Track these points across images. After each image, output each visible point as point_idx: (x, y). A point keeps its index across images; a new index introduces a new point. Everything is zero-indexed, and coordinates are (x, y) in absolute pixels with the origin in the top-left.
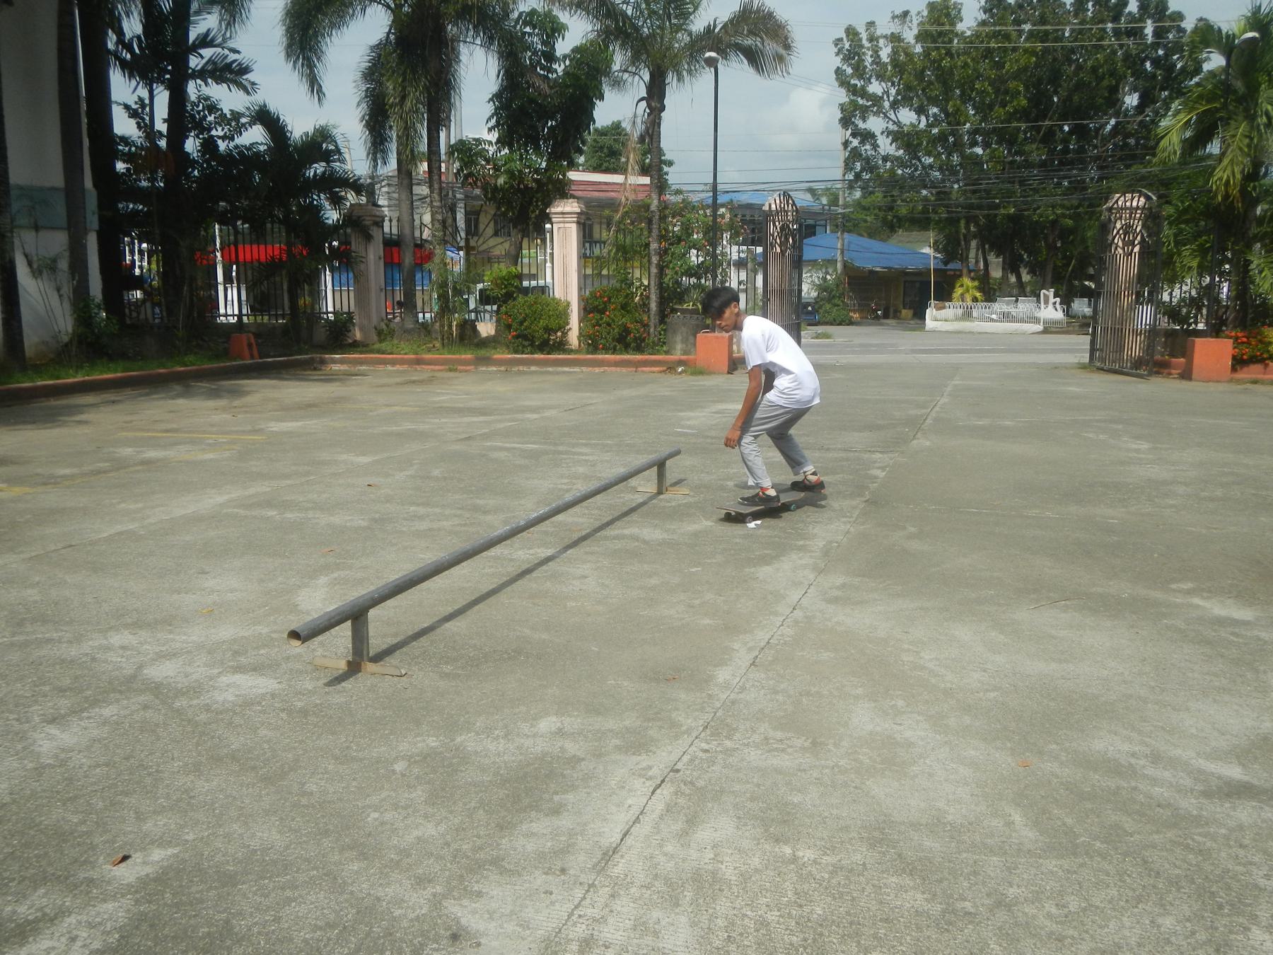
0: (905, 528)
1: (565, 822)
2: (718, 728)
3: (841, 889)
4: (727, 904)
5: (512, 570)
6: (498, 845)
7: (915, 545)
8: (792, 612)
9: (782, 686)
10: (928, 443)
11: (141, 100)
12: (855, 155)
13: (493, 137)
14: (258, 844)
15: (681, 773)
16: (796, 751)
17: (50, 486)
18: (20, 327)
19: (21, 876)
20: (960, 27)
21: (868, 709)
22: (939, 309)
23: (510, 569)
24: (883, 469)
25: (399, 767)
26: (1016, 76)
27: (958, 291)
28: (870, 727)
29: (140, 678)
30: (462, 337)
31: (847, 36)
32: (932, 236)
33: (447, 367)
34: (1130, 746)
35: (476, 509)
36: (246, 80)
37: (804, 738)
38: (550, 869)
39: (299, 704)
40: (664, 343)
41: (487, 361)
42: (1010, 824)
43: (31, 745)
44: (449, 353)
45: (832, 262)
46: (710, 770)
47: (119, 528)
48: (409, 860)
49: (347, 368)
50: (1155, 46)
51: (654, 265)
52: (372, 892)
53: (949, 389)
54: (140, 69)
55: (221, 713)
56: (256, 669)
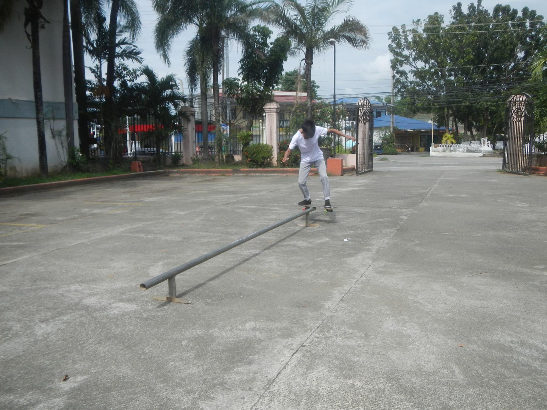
0: (414, 241)
1: (253, 367)
2: (324, 328)
3: (373, 400)
4: (321, 405)
5: (240, 259)
6: (223, 377)
7: (418, 249)
8: (361, 277)
9: (354, 310)
10: (427, 205)
11: (97, 65)
12: (398, 81)
13: (241, 78)
14: (122, 375)
15: (306, 347)
16: (358, 338)
17: (53, 225)
18: (46, 160)
19: (23, 386)
20: (443, 25)
21: (391, 320)
22: (436, 147)
23: (239, 259)
24: (406, 215)
25: (184, 343)
26: (468, 46)
27: (444, 139)
28: (392, 328)
29: (81, 304)
30: (227, 162)
31: (393, 31)
32: (432, 115)
33: (221, 174)
34: (511, 338)
35: (228, 233)
36: (139, 57)
37: (362, 333)
38: (245, 388)
39: (145, 315)
41: (238, 171)
42: (452, 372)
43: (34, 331)
44: (222, 168)
45: (388, 127)
46: (318, 346)
47: (79, 242)
48: (184, 383)
50: (531, 31)
52: (167, 396)
53: (438, 181)
54: (96, 53)
55: (112, 319)
56: (129, 300)
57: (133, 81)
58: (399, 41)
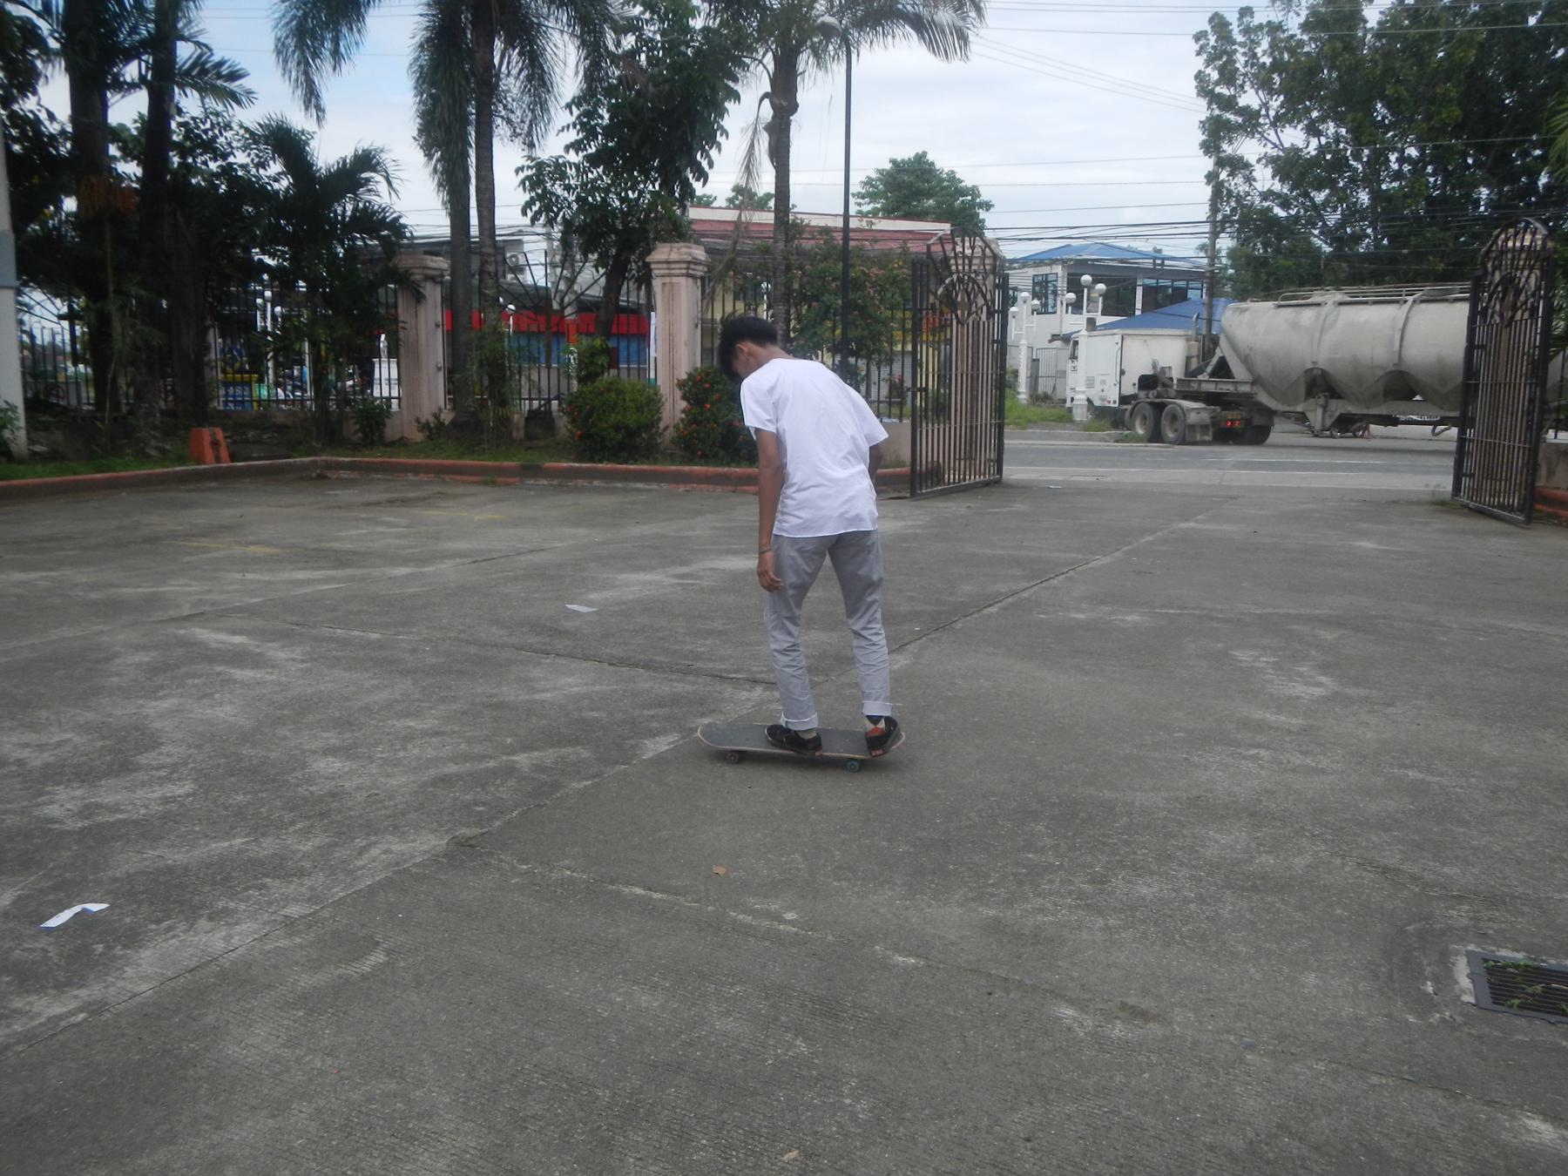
41: (532, 471)
44: (496, 460)
49: (358, 476)
57: (262, 165)
58: (1231, 61)
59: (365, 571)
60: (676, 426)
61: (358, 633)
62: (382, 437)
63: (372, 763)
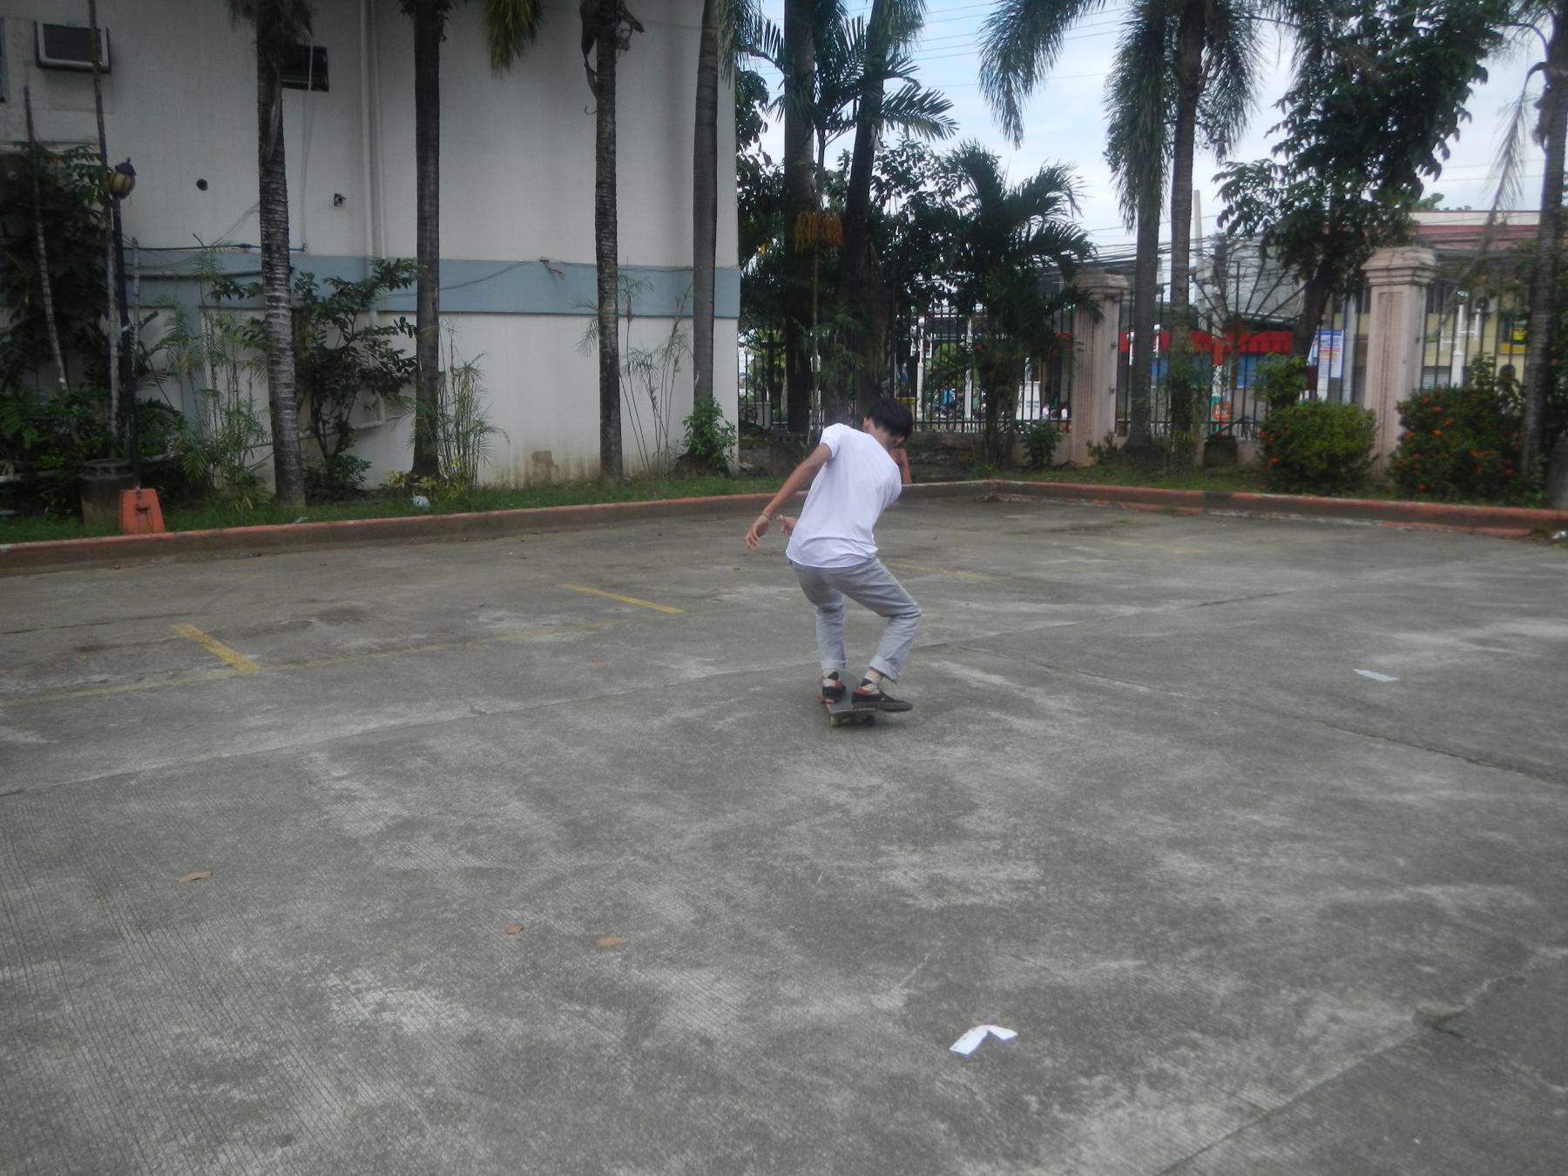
40: (1543, 487)
47: (145, 765)
51: (1538, 352)
57: (947, 193)
59: (1090, 607)
60: (1392, 456)
61: (1123, 684)
62: (1050, 461)
63: (1236, 869)
